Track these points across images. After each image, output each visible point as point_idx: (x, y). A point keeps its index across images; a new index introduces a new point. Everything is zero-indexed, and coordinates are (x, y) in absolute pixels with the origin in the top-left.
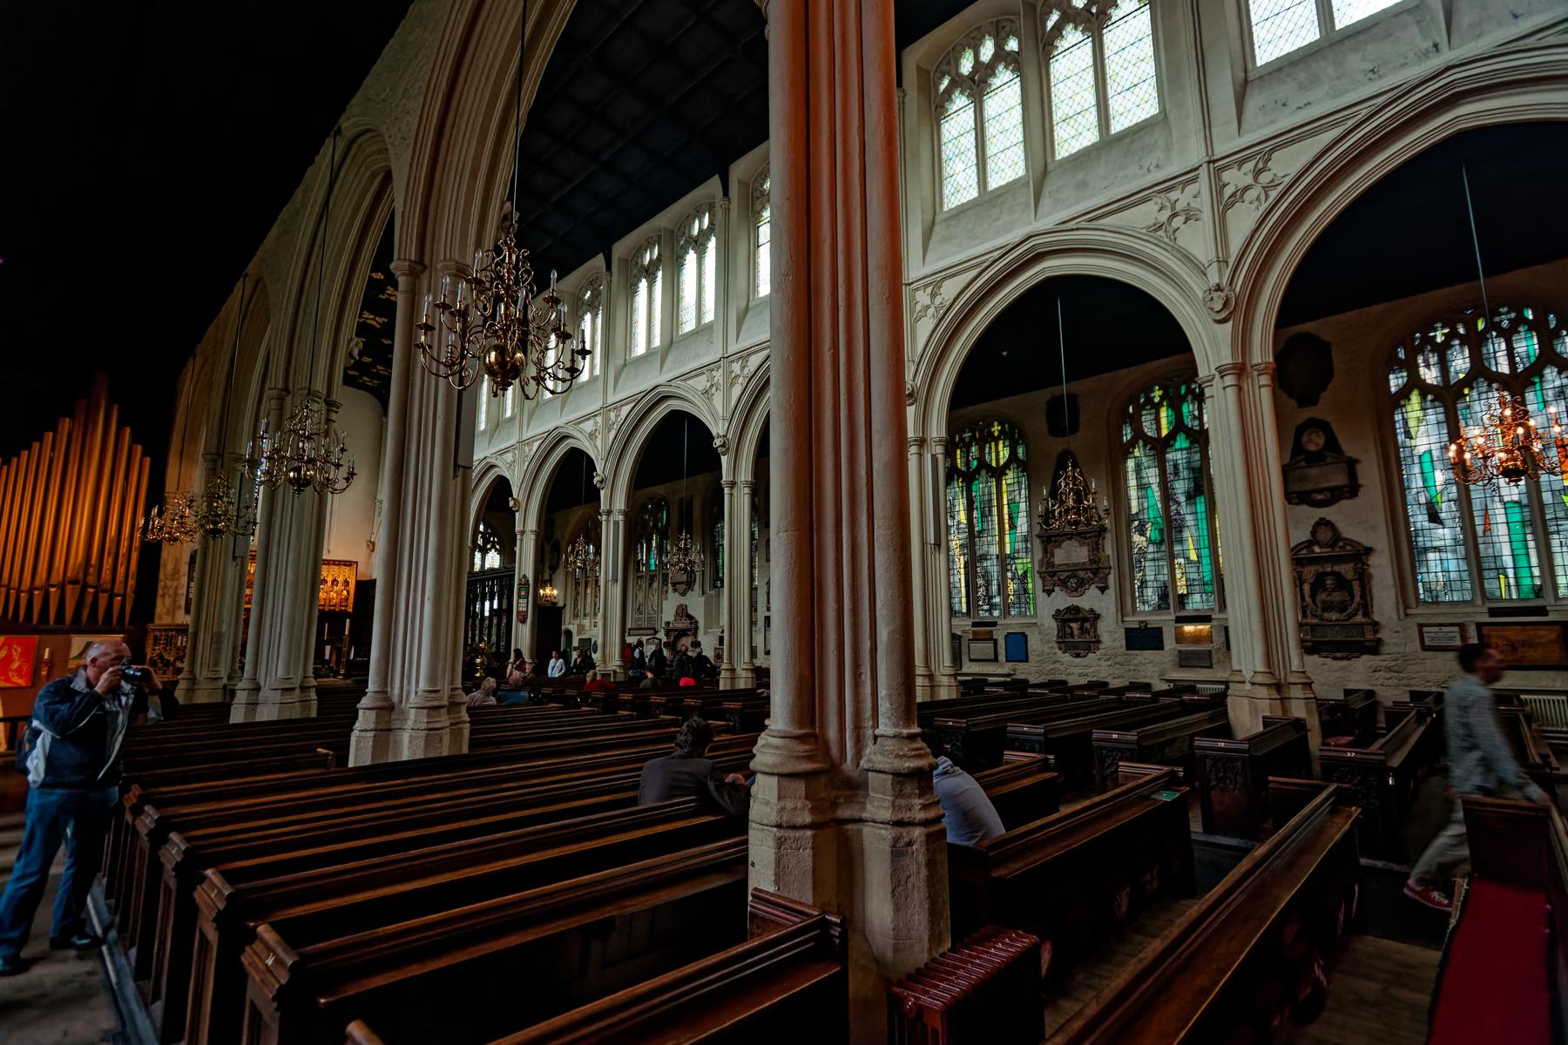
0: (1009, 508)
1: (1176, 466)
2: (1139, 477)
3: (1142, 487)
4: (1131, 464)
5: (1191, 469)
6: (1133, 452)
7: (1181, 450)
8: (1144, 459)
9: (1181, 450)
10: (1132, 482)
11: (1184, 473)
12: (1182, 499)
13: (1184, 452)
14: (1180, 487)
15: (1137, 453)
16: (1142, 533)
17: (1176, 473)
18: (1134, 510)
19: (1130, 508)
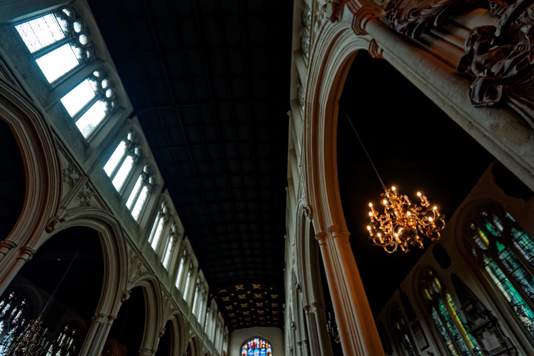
0: (459, 316)
1: (507, 262)
2: (498, 277)
3: (502, 282)
4: (488, 269)
5: (516, 261)
6: (484, 263)
7: (503, 251)
8: (492, 264)
9: (503, 251)
10: (497, 281)
11: (515, 266)
12: (526, 282)
13: (506, 252)
14: (519, 274)
15: (487, 262)
16: (524, 316)
17: (511, 267)
18: (509, 299)
19: (505, 298)
